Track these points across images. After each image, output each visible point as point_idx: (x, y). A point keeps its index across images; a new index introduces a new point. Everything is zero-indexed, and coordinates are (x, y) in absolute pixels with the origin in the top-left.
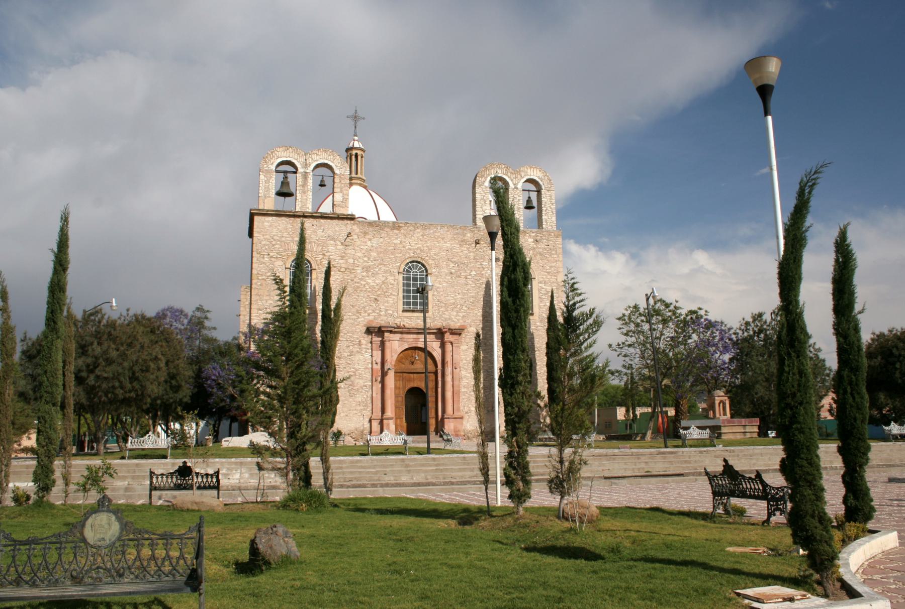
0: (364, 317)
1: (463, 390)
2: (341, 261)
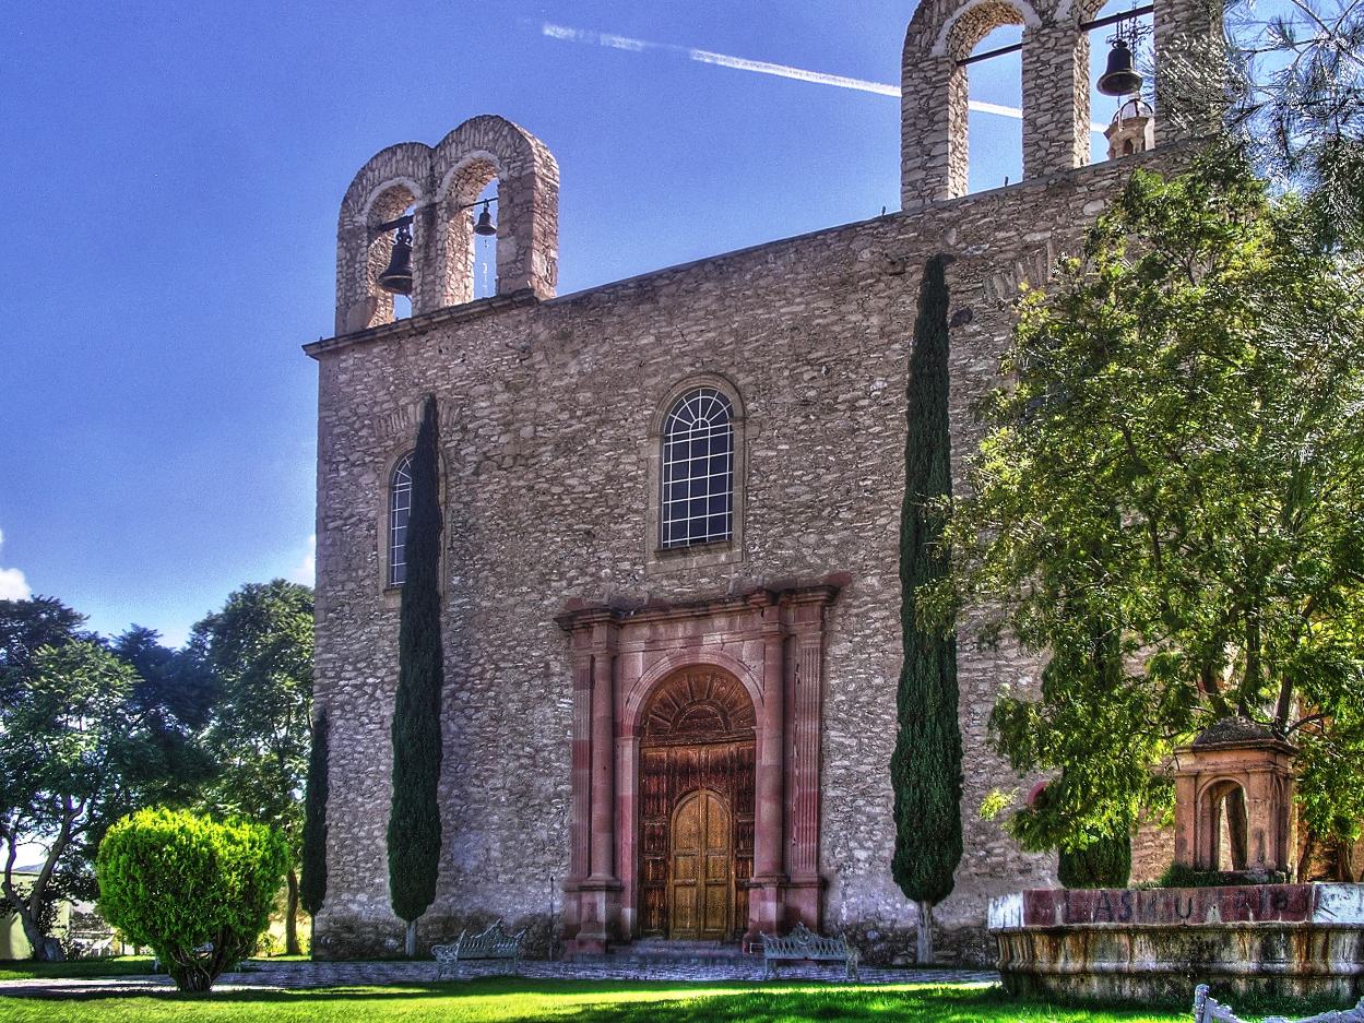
0: (557, 592)
1: (831, 793)
2: (503, 439)
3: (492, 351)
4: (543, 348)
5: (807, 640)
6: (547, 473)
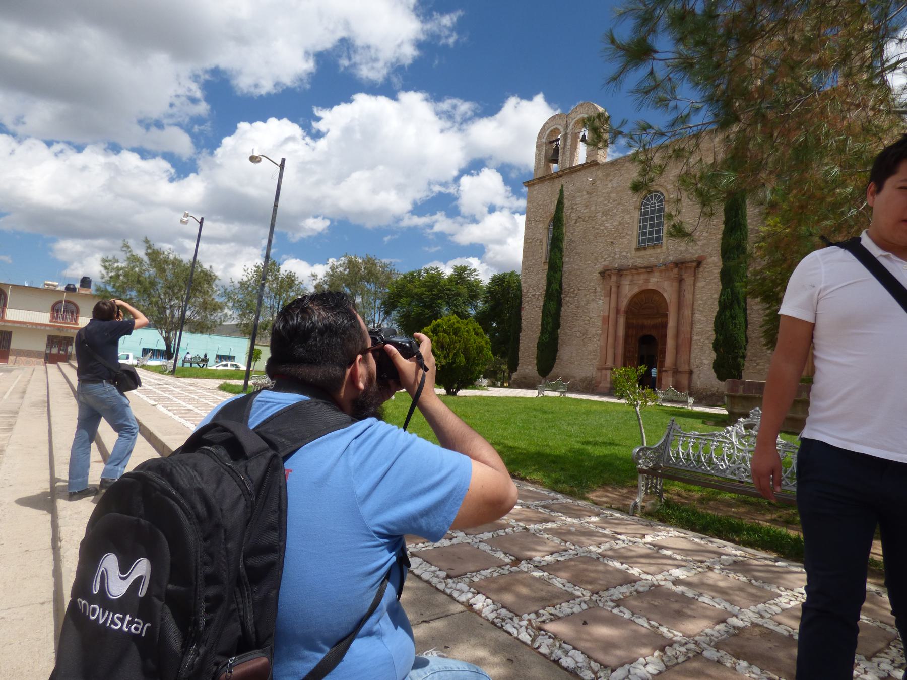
1: (695, 338)
5: (689, 281)
6: (599, 222)
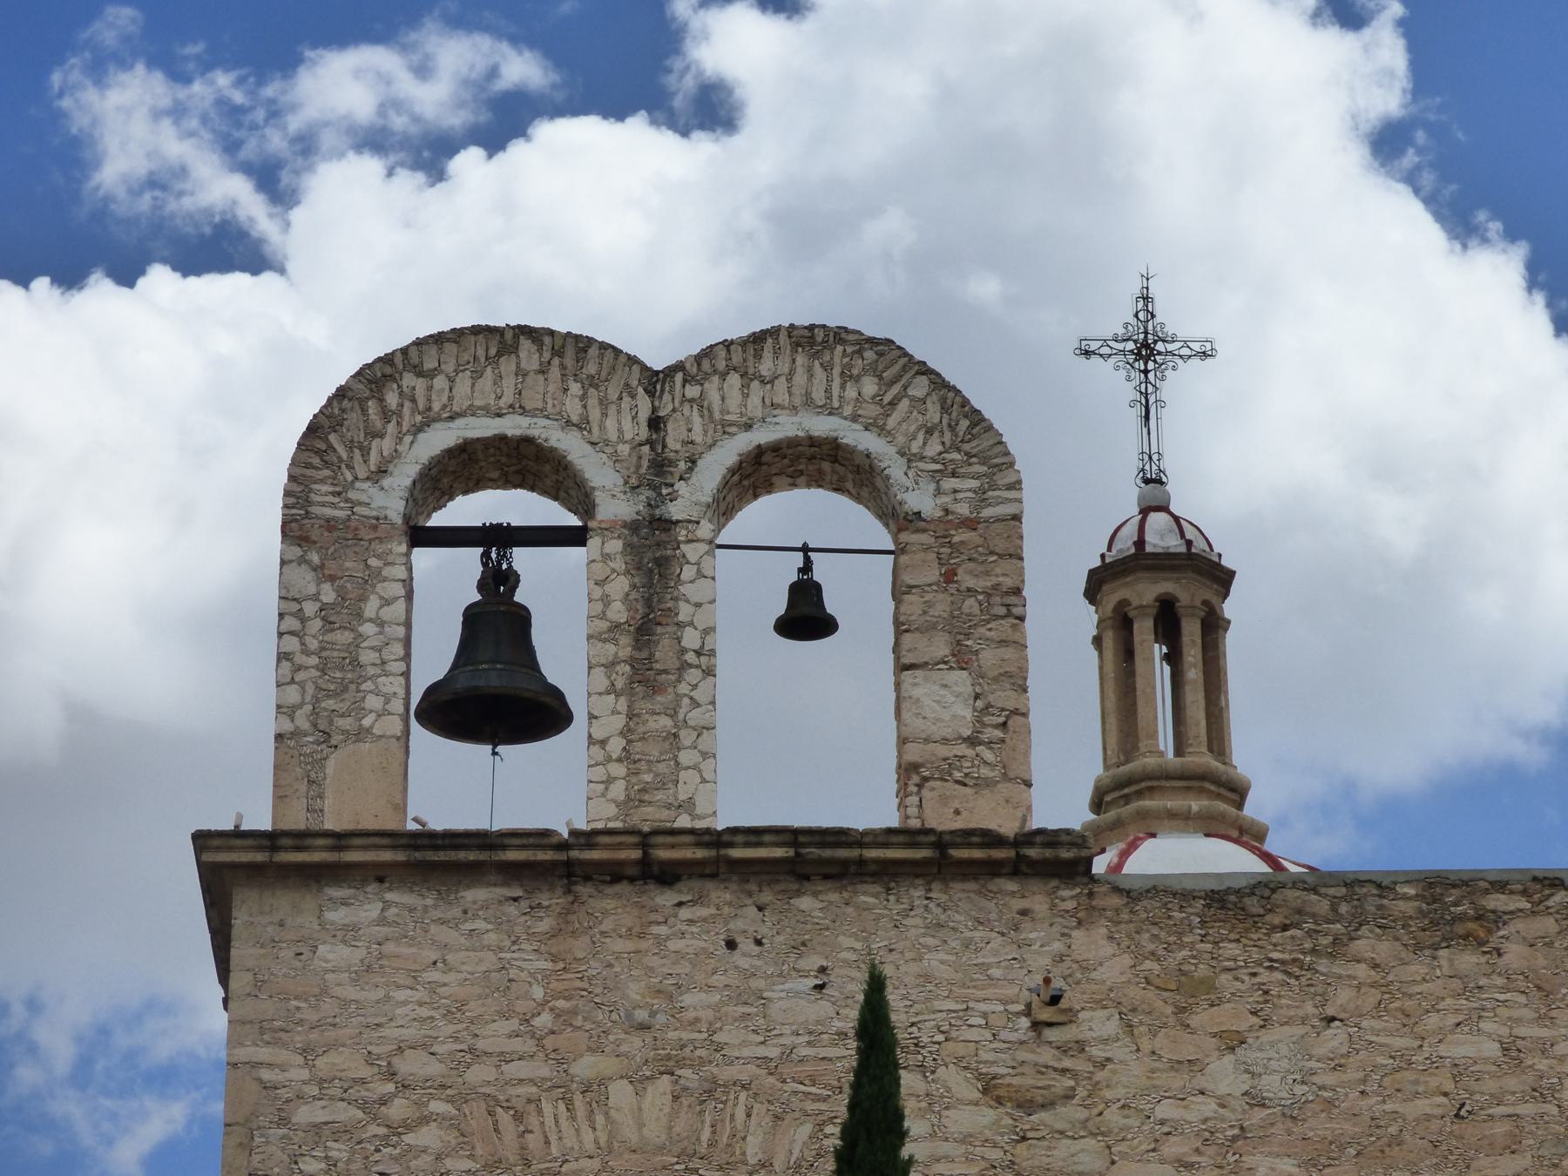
3: (927, 977)
4: (1105, 1000)
